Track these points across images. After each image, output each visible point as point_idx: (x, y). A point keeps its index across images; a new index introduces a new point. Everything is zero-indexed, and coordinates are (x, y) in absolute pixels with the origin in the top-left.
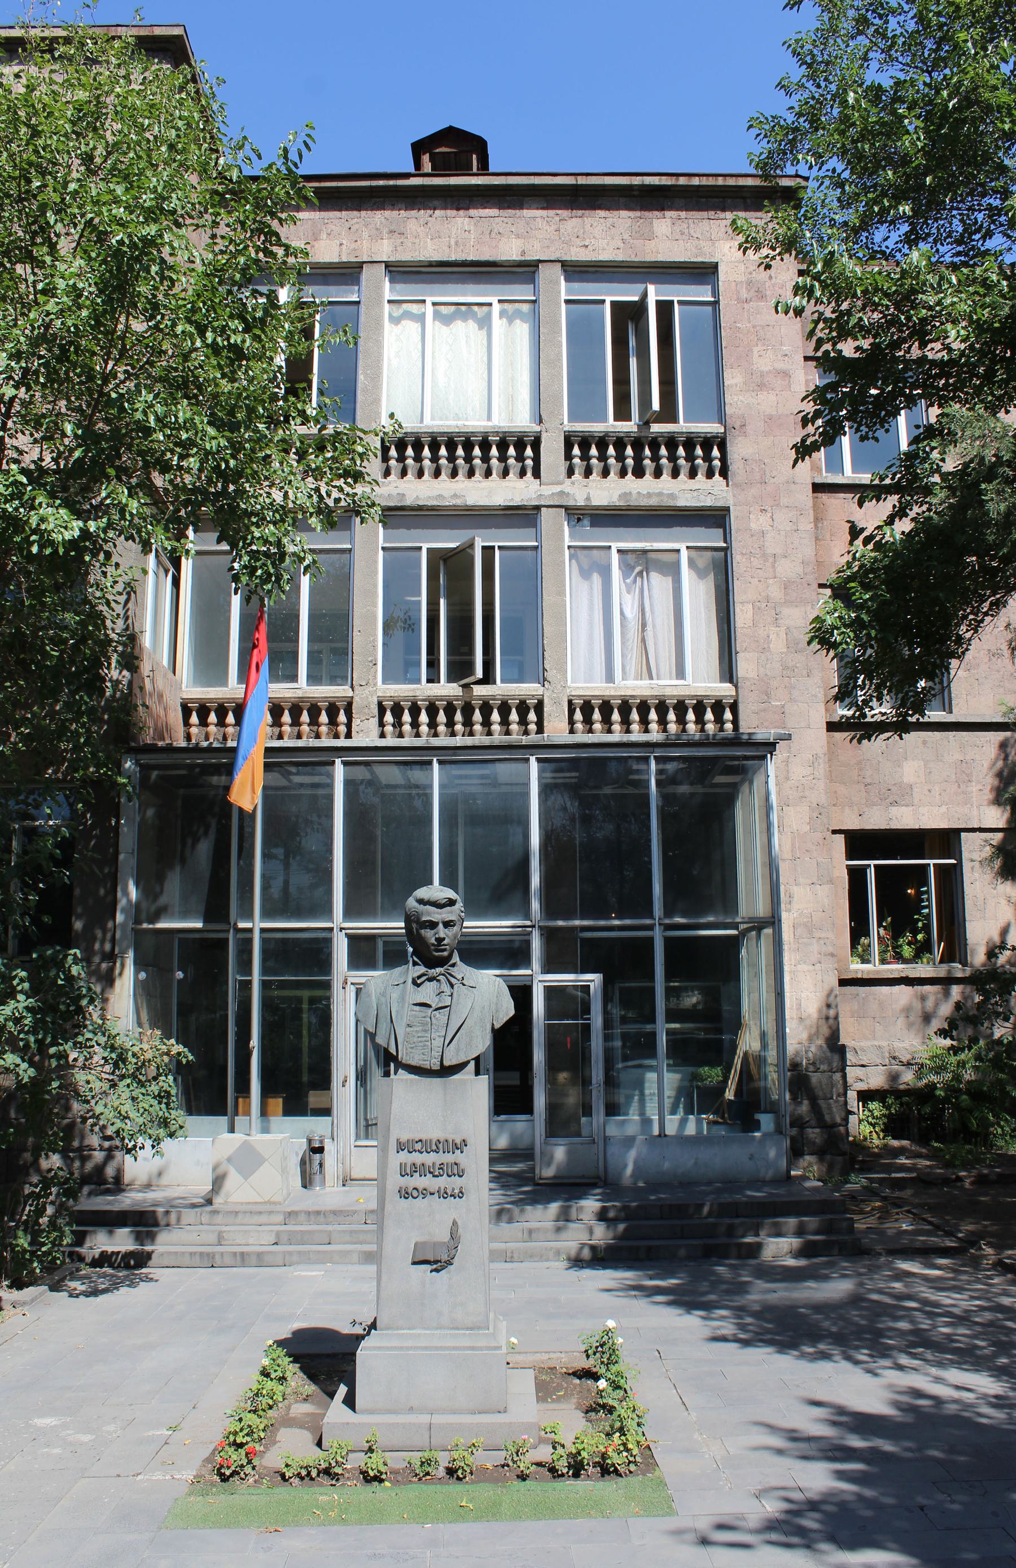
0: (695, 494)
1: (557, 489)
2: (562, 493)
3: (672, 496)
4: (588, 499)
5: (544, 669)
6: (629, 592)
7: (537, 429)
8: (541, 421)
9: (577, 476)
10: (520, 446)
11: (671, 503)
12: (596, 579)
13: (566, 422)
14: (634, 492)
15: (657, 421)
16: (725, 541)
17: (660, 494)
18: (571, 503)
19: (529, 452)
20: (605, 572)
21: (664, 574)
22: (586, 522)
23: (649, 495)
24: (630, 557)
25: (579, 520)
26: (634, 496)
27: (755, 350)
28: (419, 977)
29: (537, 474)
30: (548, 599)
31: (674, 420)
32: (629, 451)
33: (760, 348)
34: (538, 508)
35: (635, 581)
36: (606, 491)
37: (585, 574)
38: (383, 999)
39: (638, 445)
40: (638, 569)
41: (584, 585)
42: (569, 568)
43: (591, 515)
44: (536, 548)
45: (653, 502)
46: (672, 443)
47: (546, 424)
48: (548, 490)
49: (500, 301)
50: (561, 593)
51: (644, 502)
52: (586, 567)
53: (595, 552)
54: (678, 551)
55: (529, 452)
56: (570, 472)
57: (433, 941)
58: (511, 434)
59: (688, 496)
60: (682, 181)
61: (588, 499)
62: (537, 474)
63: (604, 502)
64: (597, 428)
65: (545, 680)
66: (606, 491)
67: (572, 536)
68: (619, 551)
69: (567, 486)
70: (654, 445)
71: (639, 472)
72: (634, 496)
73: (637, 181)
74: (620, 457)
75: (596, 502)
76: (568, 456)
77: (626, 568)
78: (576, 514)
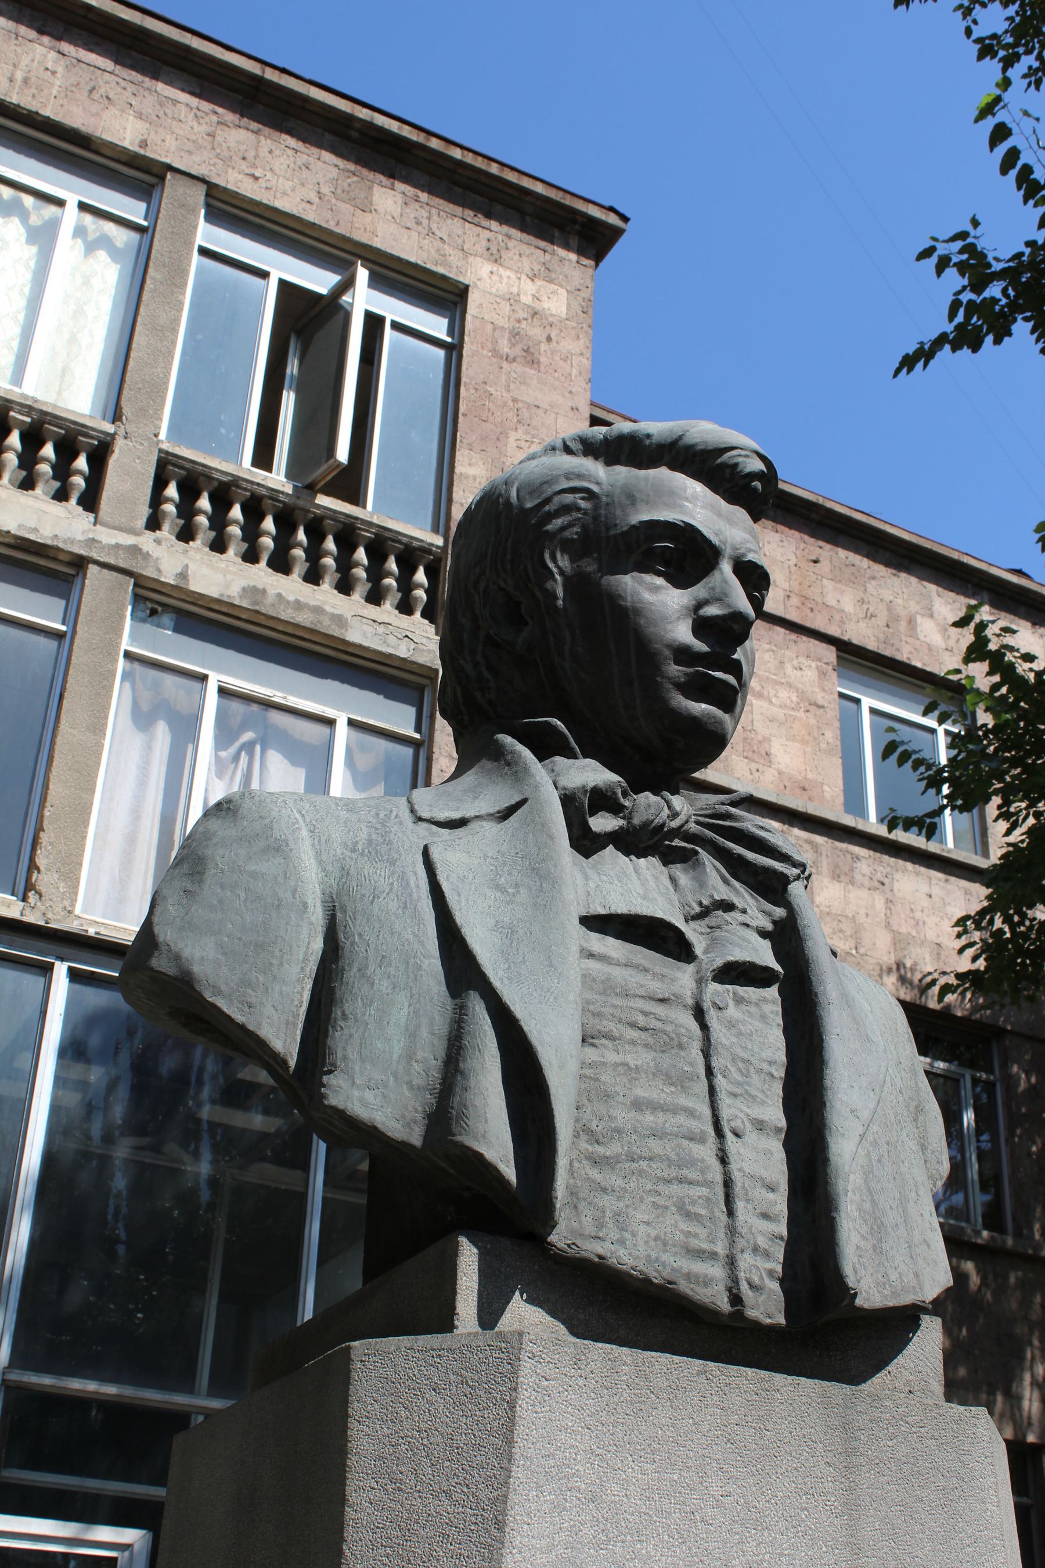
0: (381, 629)
1: (128, 540)
2: (135, 550)
3: (339, 620)
4: (183, 575)
5: (33, 866)
6: (220, 775)
7: (110, 428)
8: (117, 417)
9: (166, 532)
10: (67, 450)
11: (336, 632)
12: (162, 733)
13: (163, 435)
14: (272, 592)
15: (328, 491)
16: (418, 729)
17: (318, 610)
18: (149, 572)
19: (81, 463)
20: (186, 730)
21: (294, 762)
22: (167, 619)
23: (298, 605)
24: (236, 706)
25: (153, 612)
26: (270, 598)
27: (513, 436)
28: (602, 800)
29: (90, 501)
30: (70, 731)
31: (356, 496)
32: (268, 524)
33: (520, 434)
34: (80, 563)
35: (236, 758)
36: (218, 575)
37: (142, 719)
38: (378, 875)
39: (286, 523)
40: (248, 736)
41: (137, 740)
42: (119, 698)
43: (179, 612)
44: (59, 636)
45: (304, 619)
46: (348, 535)
47: (129, 425)
48: (108, 537)
49: (83, 207)
50: (98, 728)
51: (287, 614)
52: (145, 707)
53: (169, 679)
54: (331, 723)
55: (81, 463)
56: (154, 523)
57: (683, 633)
58: (57, 420)
59: (369, 629)
60: (434, 144)
61: (183, 575)
62: (90, 501)
63: (213, 592)
64: (219, 464)
65: (29, 886)
66: (218, 575)
67: (133, 636)
68: (223, 691)
69: (146, 541)
70: (316, 534)
71: (281, 564)
72: (270, 598)
73: (363, 113)
74: (251, 532)
75: (196, 585)
76: (157, 499)
77: (225, 733)
78: (156, 601)
